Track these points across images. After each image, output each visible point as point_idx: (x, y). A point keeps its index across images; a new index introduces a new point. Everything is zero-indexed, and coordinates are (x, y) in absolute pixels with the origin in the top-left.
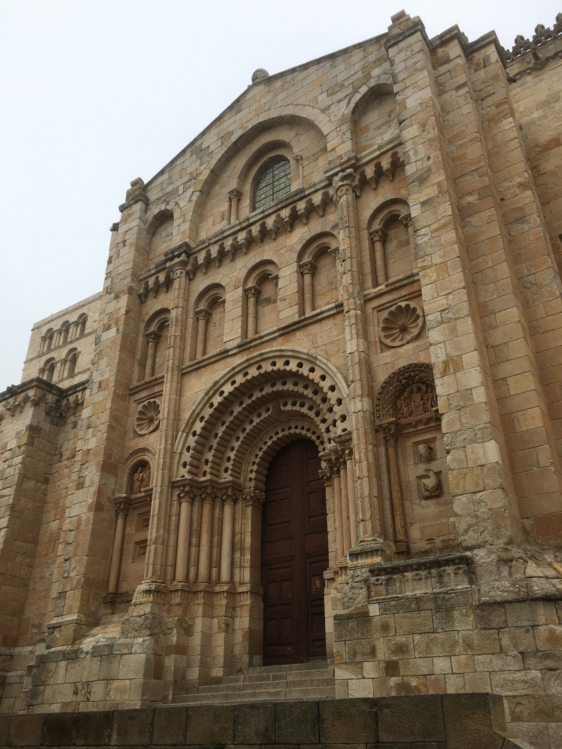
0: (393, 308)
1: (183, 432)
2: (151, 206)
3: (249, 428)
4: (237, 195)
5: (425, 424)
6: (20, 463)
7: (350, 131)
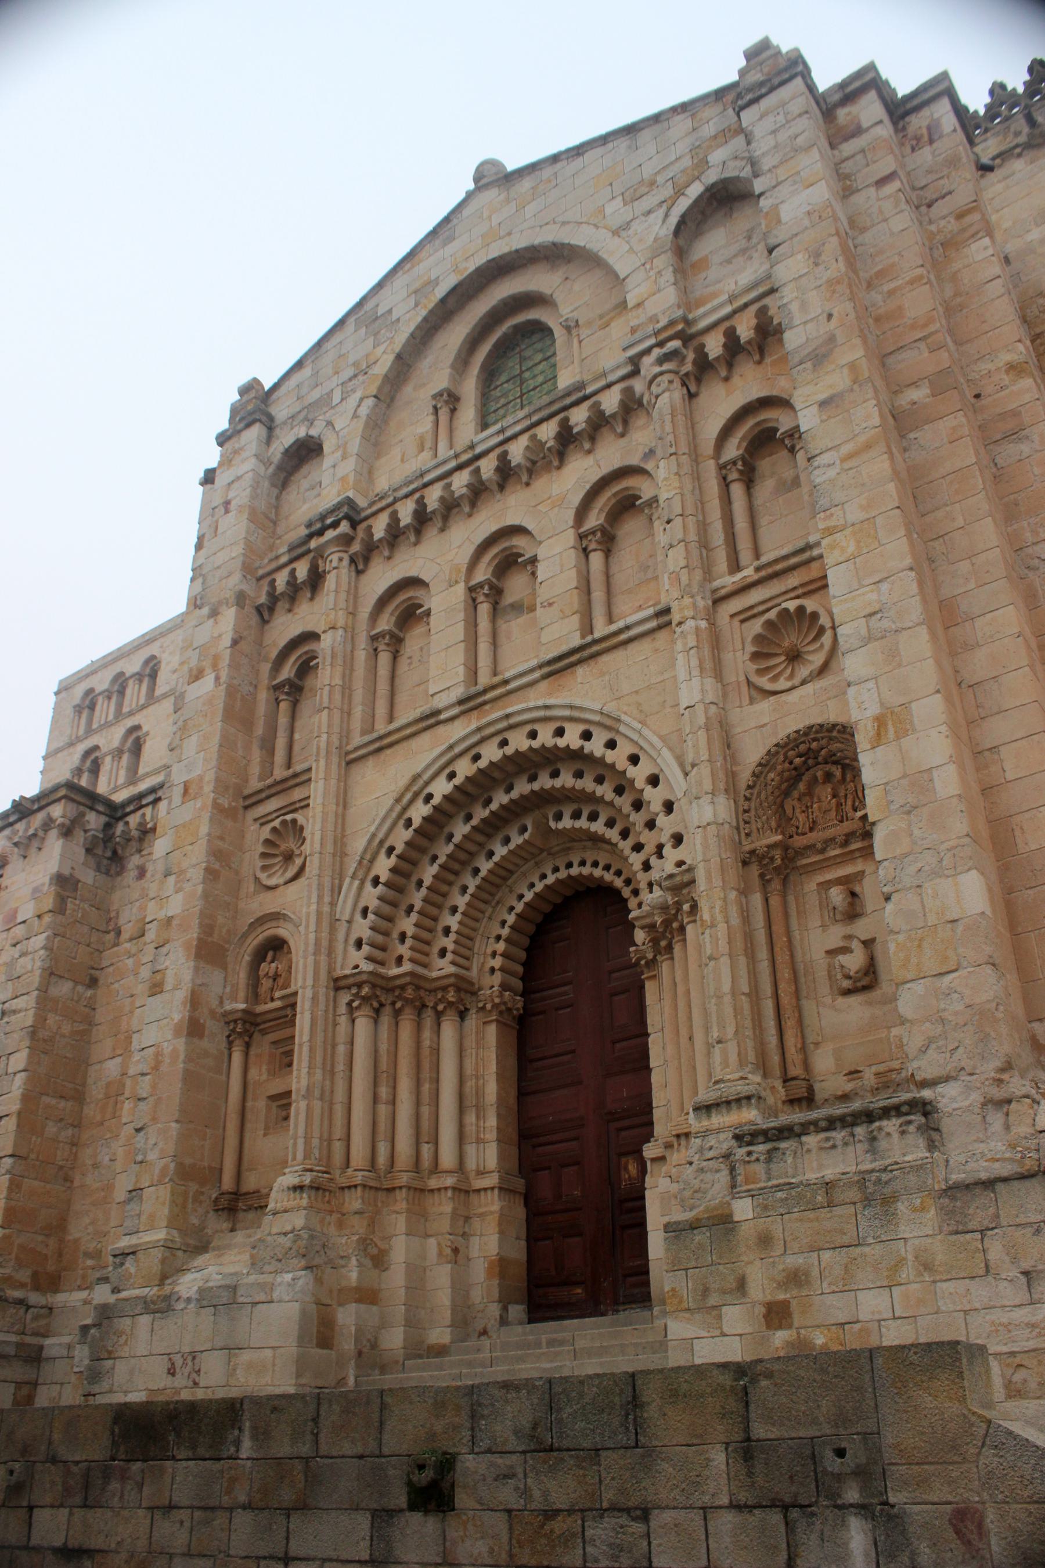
0: (772, 615)
1: (353, 877)
2: (278, 431)
3: (485, 866)
4: (451, 400)
6: (42, 948)
7: (671, 269)
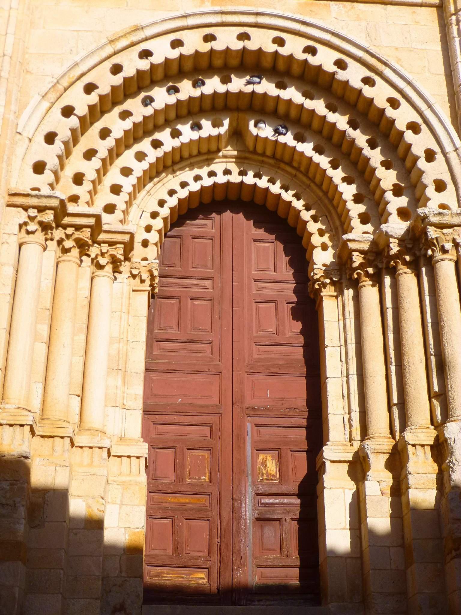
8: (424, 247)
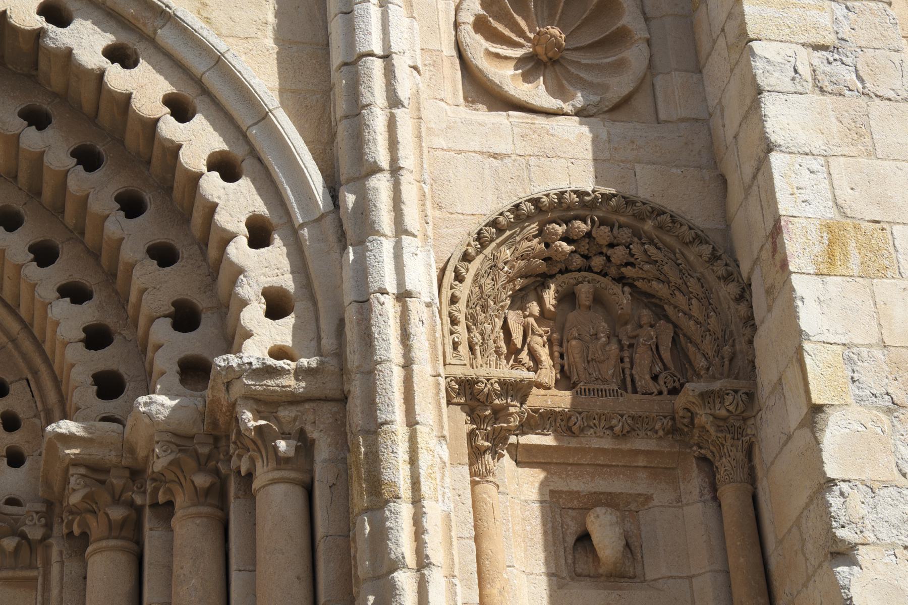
5: (616, 436)
8: (236, 452)
